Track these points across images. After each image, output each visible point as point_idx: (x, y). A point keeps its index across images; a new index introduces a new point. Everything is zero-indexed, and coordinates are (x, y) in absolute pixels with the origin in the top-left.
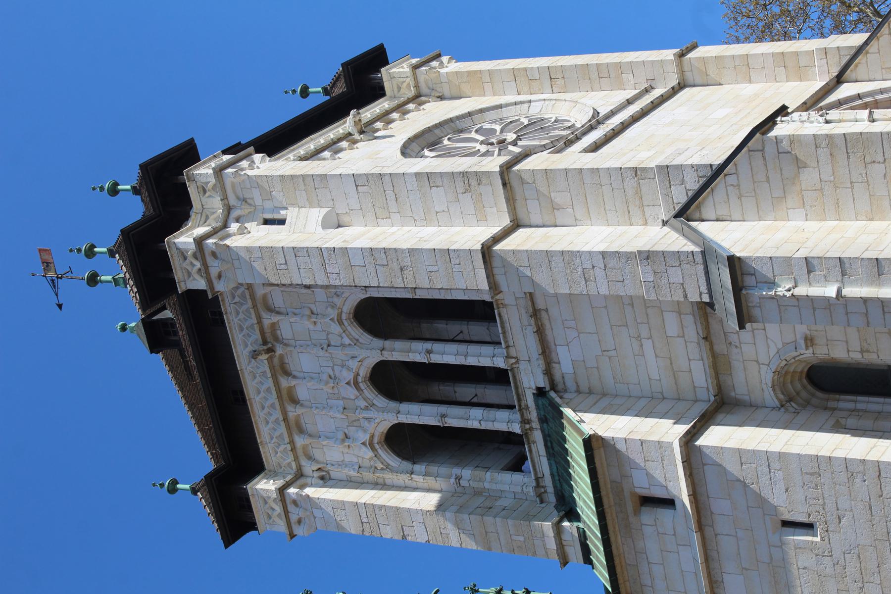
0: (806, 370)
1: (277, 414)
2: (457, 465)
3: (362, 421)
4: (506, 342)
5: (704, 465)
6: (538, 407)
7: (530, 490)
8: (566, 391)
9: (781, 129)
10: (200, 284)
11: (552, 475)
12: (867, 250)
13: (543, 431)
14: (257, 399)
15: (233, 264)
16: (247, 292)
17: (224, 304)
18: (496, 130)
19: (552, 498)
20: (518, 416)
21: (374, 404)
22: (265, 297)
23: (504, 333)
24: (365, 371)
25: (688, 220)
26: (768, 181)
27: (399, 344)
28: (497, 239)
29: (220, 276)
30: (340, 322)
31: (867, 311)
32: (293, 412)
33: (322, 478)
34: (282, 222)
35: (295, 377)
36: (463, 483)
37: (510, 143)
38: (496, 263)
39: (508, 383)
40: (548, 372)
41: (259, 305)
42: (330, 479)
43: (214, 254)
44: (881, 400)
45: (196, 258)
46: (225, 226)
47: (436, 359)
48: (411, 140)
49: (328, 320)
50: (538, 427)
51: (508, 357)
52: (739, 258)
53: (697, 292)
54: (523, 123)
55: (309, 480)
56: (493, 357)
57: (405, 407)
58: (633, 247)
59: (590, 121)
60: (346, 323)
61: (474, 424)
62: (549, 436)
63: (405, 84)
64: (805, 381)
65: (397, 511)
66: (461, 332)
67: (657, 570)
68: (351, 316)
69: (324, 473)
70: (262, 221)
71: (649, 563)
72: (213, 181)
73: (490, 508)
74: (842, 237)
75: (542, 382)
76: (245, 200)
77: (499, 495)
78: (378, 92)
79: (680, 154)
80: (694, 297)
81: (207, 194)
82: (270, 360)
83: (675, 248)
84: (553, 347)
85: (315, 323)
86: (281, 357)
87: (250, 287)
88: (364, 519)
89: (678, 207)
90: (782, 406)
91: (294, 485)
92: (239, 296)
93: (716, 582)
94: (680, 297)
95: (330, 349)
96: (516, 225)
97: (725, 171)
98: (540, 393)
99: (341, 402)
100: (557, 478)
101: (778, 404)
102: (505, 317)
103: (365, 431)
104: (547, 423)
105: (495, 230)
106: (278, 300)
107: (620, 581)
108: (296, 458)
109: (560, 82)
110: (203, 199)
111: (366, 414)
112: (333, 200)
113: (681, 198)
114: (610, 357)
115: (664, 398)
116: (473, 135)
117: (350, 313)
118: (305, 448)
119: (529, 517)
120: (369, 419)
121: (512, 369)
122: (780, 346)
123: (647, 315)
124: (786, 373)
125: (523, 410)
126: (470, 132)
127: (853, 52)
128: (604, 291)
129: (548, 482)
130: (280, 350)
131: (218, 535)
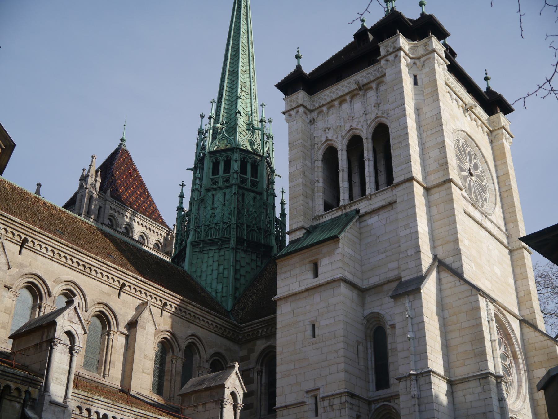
0: (382, 326)
1: (334, 96)
2: (324, 180)
3: (336, 135)
4: (377, 193)
5: (333, 288)
6: (352, 211)
7: (317, 213)
8: (360, 223)
9: (482, 302)
10: (383, 52)
11: (324, 222)
12: (431, 347)
13: (342, 215)
14: (340, 87)
15: (393, 65)
16: (383, 74)
17: (377, 64)
18: (478, 170)
19: (315, 224)
20: (347, 202)
21: (344, 139)
22: (383, 82)
24: (357, 132)
27: (370, 145)
29: (387, 61)
30: (377, 117)
31: (404, 351)
32: (336, 103)
33: (310, 121)
35: (351, 102)
36: (316, 184)
37: (471, 178)
38: (408, 184)
39: (362, 196)
40: (366, 214)
41: (379, 80)
42: (311, 125)
43: (396, 56)
44: (373, 359)
45: (394, 49)
48: (467, 133)
49: (377, 112)
50: (344, 213)
51: (371, 195)
52: (420, 292)
54: (483, 182)
55: (309, 116)
56: (370, 188)
57: (345, 153)
59: (486, 213)
61: (341, 185)
62: (340, 218)
63: (495, 124)
64: (377, 326)
66: (381, 172)
67: (288, 274)
68: (380, 122)
69: (313, 122)
70: (415, 74)
71: (291, 270)
72: (430, 49)
73: (307, 198)
74: (437, 336)
75: (362, 212)
76: (423, 65)
77: (313, 200)
78: (490, 111)
79: (468, 258)
80: (403, 274)
81: (424, 47)
82: (356, 89)
83: (423, 262)
84: (378, 214)
85: (375, 106)
86: (358, 94)
87: (385, 75)
88: (294, 144)
89: (444, 261)
90: (365, 318)
91: (305, 110)
92: (382, 70)
93: (287, 300)
95: (364, 115)
97: (461, 280)
98: (358, 211)
99: (343, 124)
100: (323, 224)
101: (365, 315)
102: (387, 191)
103: (332, 137)
104: (345, 216)
106: (382, 88)
107: (282, 259)
108: (317, 109)
110: (422, 46)
111: (339, 136)
112: (428, 105)
113: (448, 261)
114: (376, 240)
115: (362, 266)
116: (474, 161)
117: (381, 121)
118: (322, 111)
119: (305, 215)
120: (337, 138)
121: (366, 198)
123: (396, 254)
125: (350, 205)
127: (535, 325)
129: (322, 220)
131: (280, 81)
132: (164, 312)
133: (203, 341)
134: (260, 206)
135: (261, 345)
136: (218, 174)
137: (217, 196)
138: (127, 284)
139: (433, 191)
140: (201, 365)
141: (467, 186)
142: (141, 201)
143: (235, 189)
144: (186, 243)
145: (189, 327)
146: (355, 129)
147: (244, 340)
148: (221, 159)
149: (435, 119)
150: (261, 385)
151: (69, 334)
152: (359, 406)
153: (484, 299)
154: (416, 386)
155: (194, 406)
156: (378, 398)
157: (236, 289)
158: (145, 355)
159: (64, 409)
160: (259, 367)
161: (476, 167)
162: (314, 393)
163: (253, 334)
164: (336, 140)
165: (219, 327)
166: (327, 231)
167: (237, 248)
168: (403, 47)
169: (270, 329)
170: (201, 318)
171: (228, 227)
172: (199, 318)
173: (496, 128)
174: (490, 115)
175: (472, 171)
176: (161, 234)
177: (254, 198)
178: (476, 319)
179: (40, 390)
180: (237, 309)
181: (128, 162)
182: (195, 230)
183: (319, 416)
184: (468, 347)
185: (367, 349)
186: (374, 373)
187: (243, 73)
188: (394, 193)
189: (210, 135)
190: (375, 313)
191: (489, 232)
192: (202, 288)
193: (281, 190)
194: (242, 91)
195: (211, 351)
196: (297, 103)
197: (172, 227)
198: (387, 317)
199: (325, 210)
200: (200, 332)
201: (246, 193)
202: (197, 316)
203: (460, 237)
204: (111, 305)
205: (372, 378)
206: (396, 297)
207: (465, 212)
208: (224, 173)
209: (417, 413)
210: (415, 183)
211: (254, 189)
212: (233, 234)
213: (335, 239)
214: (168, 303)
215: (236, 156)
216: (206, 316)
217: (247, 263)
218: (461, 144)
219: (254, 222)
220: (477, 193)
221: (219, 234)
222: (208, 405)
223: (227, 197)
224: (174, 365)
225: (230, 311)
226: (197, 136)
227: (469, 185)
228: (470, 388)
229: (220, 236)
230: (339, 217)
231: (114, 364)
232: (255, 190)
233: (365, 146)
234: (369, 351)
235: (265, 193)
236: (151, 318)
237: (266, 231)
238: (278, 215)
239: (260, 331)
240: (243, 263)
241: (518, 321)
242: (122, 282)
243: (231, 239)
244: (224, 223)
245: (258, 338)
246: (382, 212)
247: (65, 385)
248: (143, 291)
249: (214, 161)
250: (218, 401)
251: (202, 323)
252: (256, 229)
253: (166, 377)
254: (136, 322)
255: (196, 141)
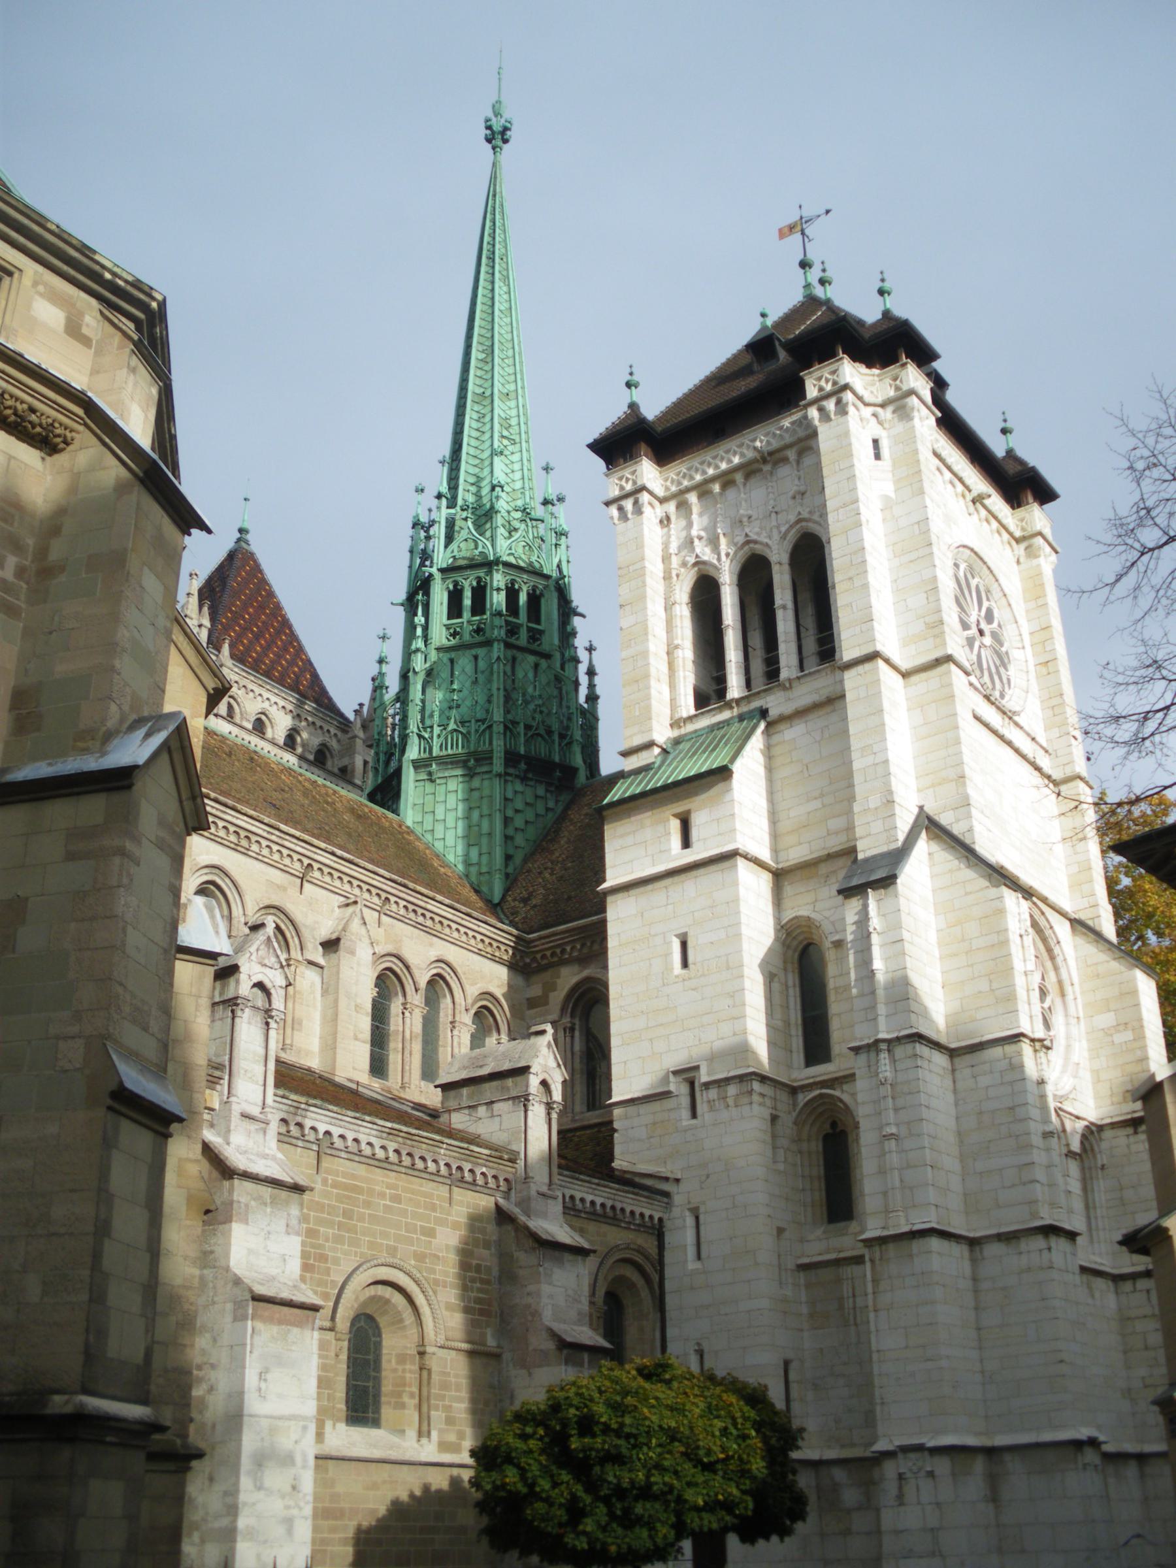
1: (711, 472)
6: (751, 712)
9: (1011, 900)
10: (812, 392)
11: (696, 731)
13: (732, 718)
14: (721, 453)
19: (676, 733)
23: (810, 674)
24: (758, 548)
25: (927, 829)
26: (967, 894)
28: (887, 661)
30: (799, 521)
33: (661, 522)
34: (878, 456)
35: (745, 484)
38: (867, 666)
40: (783, 719)
41: (803, 444)
44: (799, 1007)
46: (866, 404)
47: (780, 614)
48: (972, 550)
51: (790, 680)
52: (894, 883)
53: (866, 849)
58: (896, 785)
60: (798, 526)
65: (643, 598)
67: (630, 840)
80: (860, 846)
83: (899, 824)
86: (760, 470)
89: (936, 818)
94: (859, 832)
95: (773, 515)
96: (905, 675)
98: (764, 713)
105: (896, 659)
106: (808, 461)
109: (1044, 670)
113: (945, 820)
116: (986, 604)
122: (832, 919)
124: (809, 927)
126: (988, 599)
128: (856, 765)
129: (690, 727)
130: (767, 468)
131: (596, 435)
132: (384, 918)
133: (459, 971)
134: (548, 684)
135: (569, 978)
136: (460, 616)
137: (460, 662)
138: (316, 866)
139: (915, 679)
140: (457, 1019)
141: (974, 658)
142: (286, 660)
143: (497, 650)
144: (400, 761)
145: (431, 945)
146: (755, 542)
147: (535, 965)
148: (466, 584)
149: (917, 532)
150: (573, 1054)
151: (260, 985)
152: (775, 1099)
153: (1014, 893)
154: (887, 1061)
155: (470, 1107)
156: (811, 1081)
157: (508, 858)
158: (356, 1006)
159: (263, 1125)
160: (566, 1020)
161: (989, 617)
162: (688, 1074)
163: (553, 954)
164: (715, 562)
165: (487, 941)
166: (704, 752)
167: (506, 774)
168: (851, 384)
169: (589, 944)
170: (454, 926)
171: (484, 731)
172: (449, 926)
173: (1026, 534)
174: (1013, 508)
175: (983, 625)
176: (328, 731)
177: (536, 666)
178: (998, 932)
179: (221, 1094)
180: (514, 900)
181: (256, 577)
182: (420, 736)
183: (699, 1118)
184: (984, 985)
185: (787, 987)
186: (800, 1032)
187: (504, 398)
188: (837, 679)
189: (440, 531)
190: (801, 917)
191: (1017, 751)
192: (437, 856)
193: (587, 645)
194: (503, 437)
195: (473, 991)
196: (635, 483)
197: (351, 716)
198: (827, 927)
199: (697, 708)
200: (453, 954)
201: (519, 655)
202: (446, 922)
203: (967, 772)
204: (290, 907)
205: (798, 1043)
206: (847, 892)
207: (977, 718)
208: (474, 613)
209: (891, 1112)
210: (880, 662)
211: (535, 647)
212: (498, 745)
213: (723, 773)
214: (393, 899)
215: (499, 579)
216: (463, 922)
217: (527, 804)
218: (961, 574)
219: (537, 716)
220: (993, 670)
221: (468, 741)
222: (496, 1106)
223: (482, 664)
224: (408, 1021)
225: (499, 904)
226: (410, 532)
227: (979, 656)
228: (985, 1063)
229: (472, 749)
230: (727, 723)
231: (300, 1024)
232: (538, 649)
233: (776, 578)
234: (791, 991)
235: (557, 656)
236: (363, 931)
237: (562, 736)
238: (582, 699)
239: (568, 948)
240: (519, 805)
241: (1067, 923)
242: (306, 861)
243: (495, 755)
244: (478, 721)
245: (563, 962)
246: (811, 716)
247: (261, 1082)
248: (346, 879)
249: (451, 587)
250: (518, 1097)
251: (455, 935)
252: (542, 732)
253: (392, 1045)
254: (338, 940)
255: (408, 543)
